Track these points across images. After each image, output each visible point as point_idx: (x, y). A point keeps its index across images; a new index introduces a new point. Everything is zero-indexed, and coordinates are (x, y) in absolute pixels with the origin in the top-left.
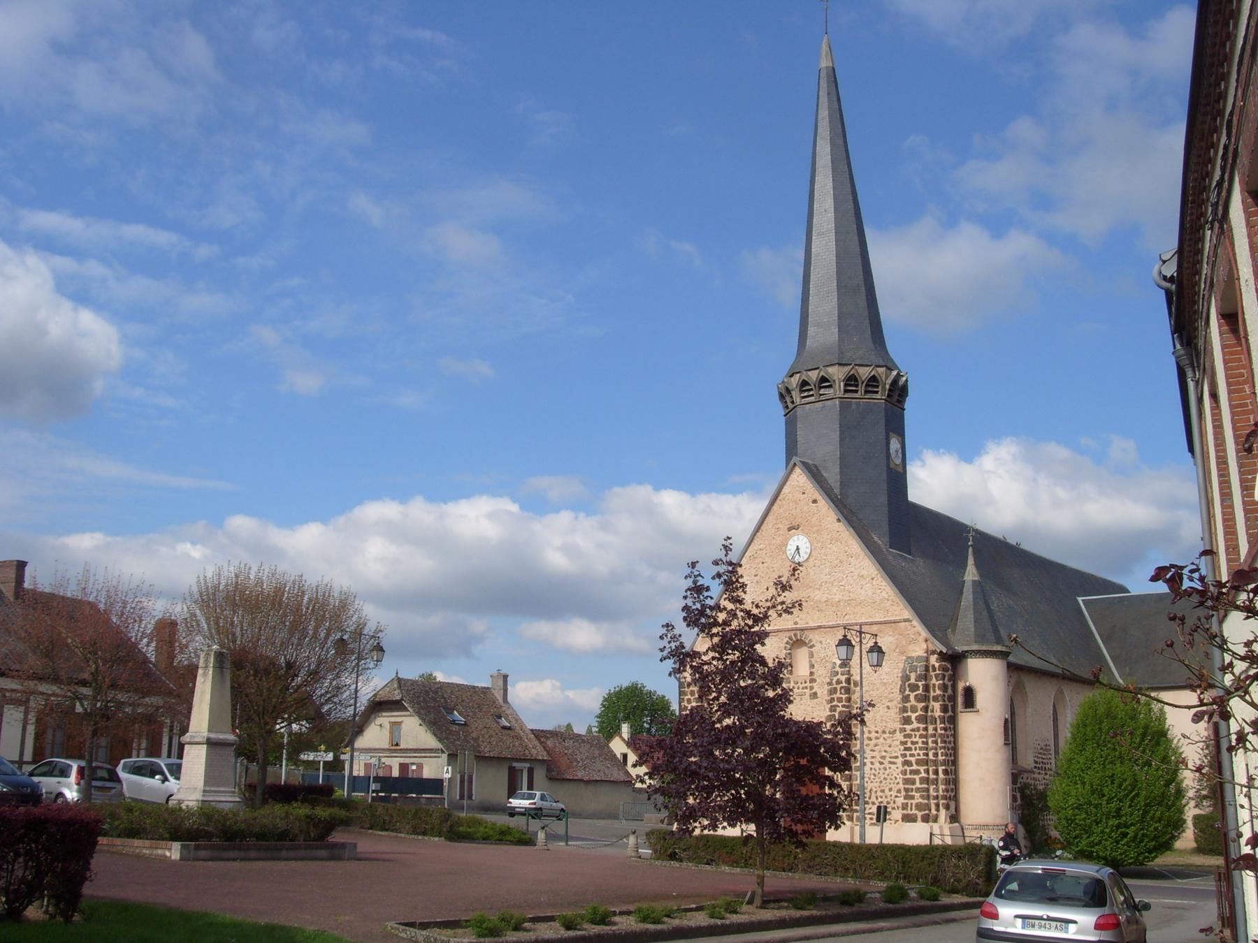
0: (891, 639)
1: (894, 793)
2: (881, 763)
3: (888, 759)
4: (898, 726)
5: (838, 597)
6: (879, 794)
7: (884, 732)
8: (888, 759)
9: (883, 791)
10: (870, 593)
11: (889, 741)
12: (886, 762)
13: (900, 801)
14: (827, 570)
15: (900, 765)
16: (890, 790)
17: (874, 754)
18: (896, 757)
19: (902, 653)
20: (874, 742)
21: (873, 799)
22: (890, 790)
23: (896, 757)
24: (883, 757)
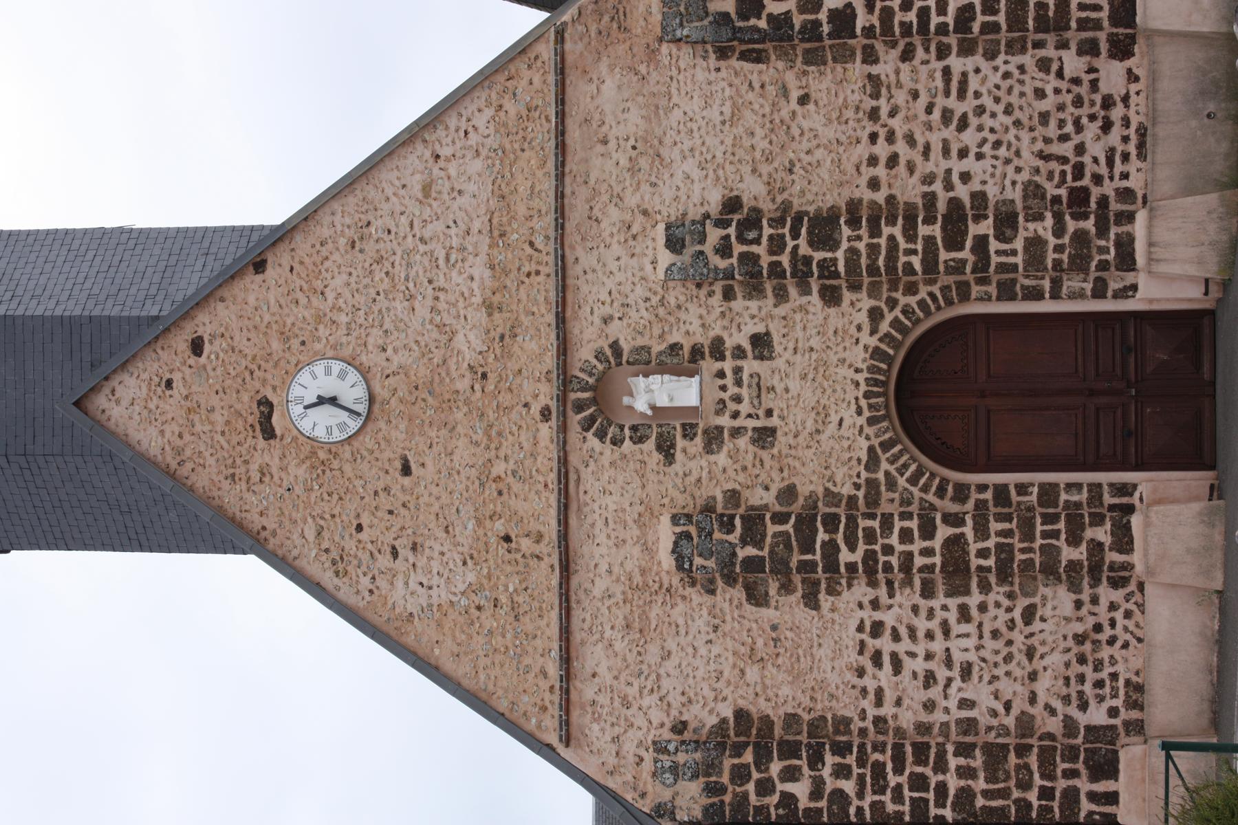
0: (609, 87)
1: (1051, 83)
2: (963, 124)
3: (952, 102)
4: (857, 69)
5: (479, 269)
6: (1052, 131)
7: (874, 114)
8: (952, 102)
9: (1044, 117)
10: (477, 165)
11: (901, 97)
12: (960, 108)
13: (1073, 63)
14: (400, 306)
15: (969, 63)
16: (1040, 94)
17: (937, 148)
18: (947, 72)
19: (652, 53)
20: (901, 147)
21: (1067, 149)
22: (1040, 94)
23: (947, 72)
24: (947, 116)
